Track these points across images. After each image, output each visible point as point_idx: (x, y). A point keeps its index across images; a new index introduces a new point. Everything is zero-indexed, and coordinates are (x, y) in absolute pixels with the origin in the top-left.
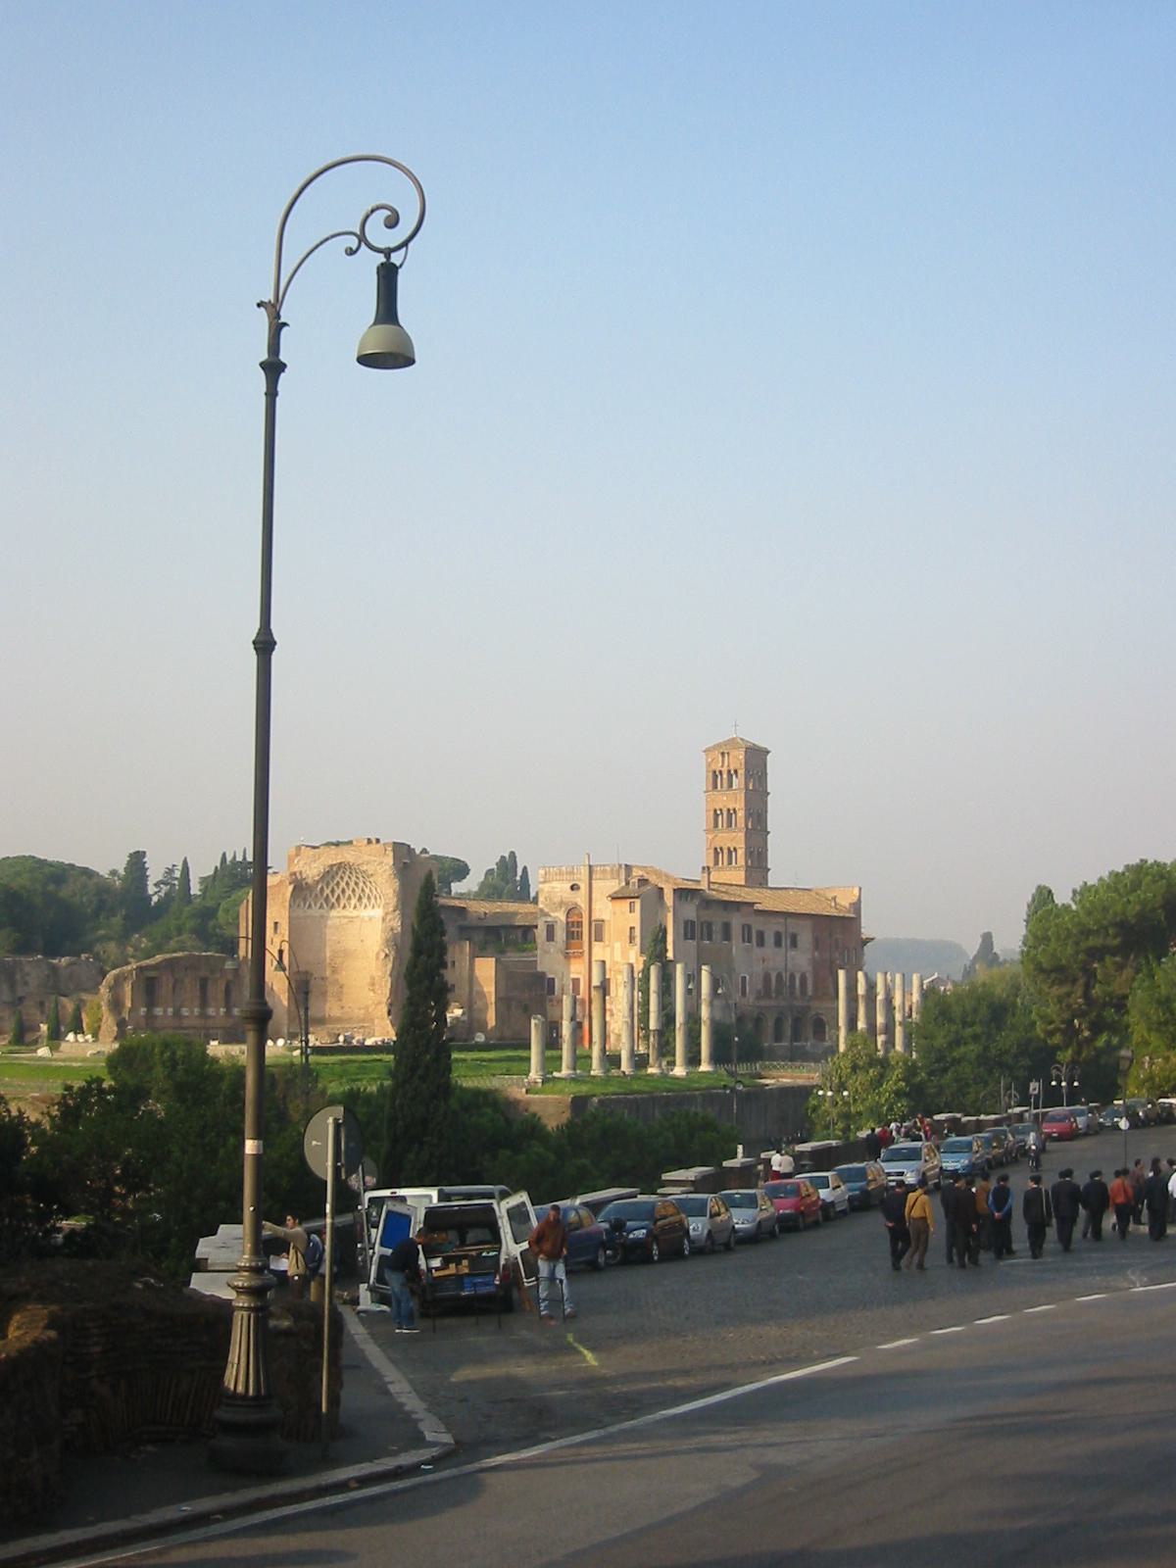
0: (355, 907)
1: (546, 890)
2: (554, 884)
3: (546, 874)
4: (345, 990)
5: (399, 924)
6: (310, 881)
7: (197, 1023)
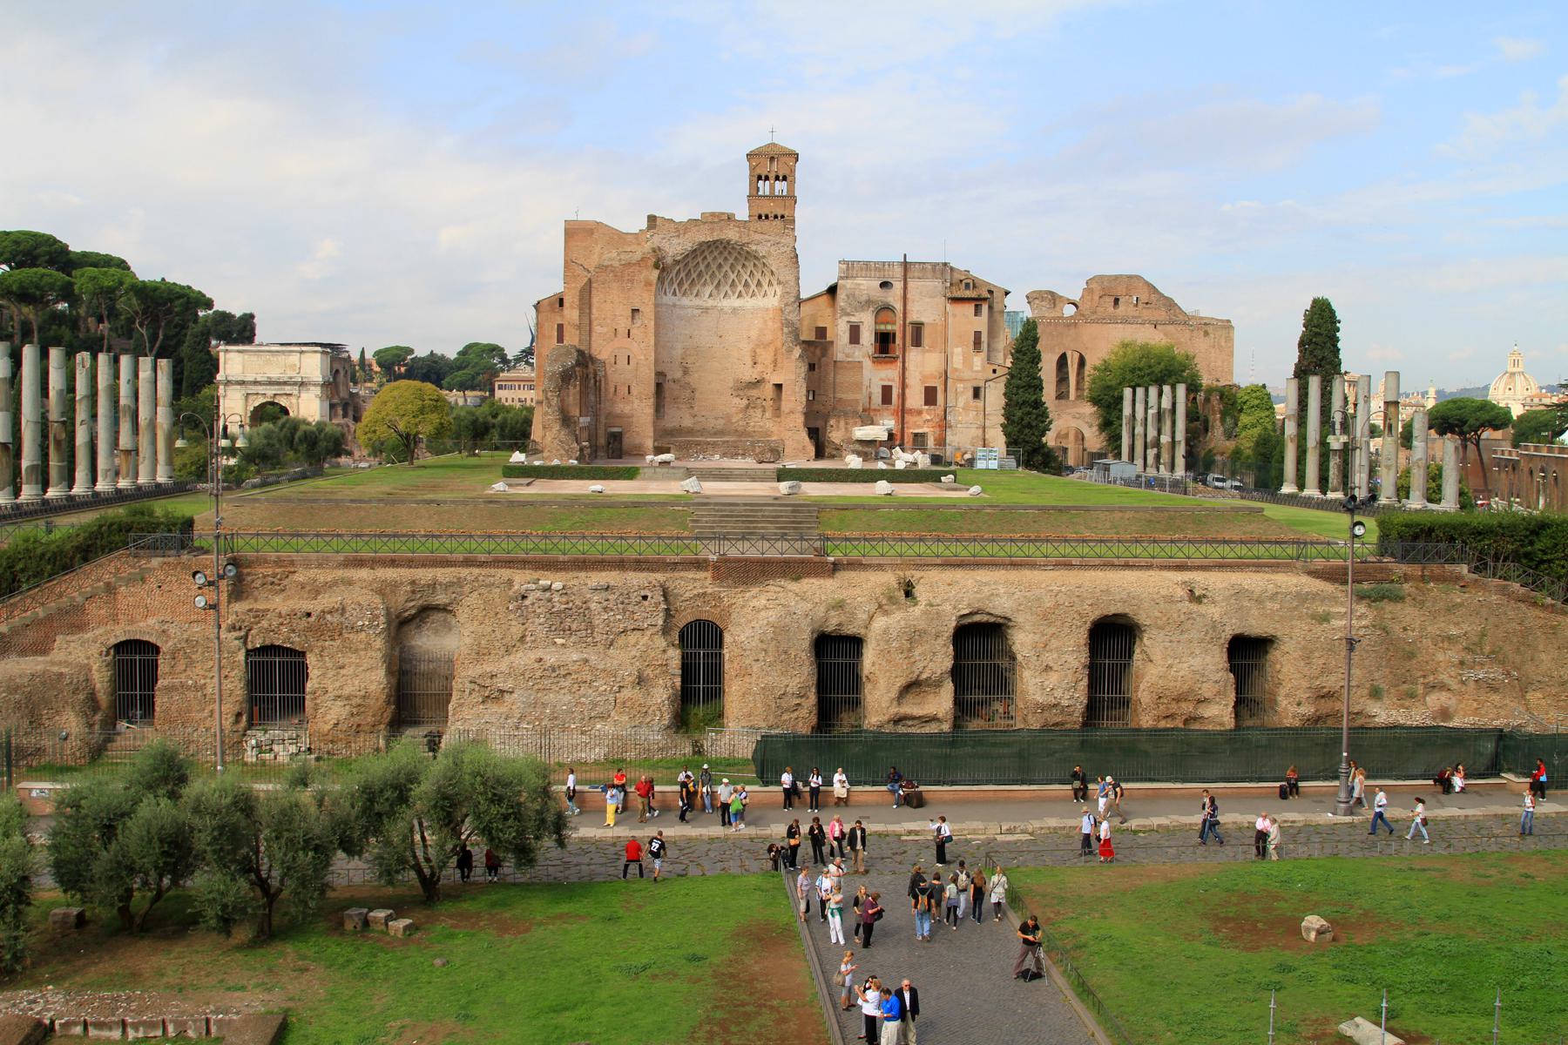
0: (710, 295)
1: (848, 286)
2: (859, 281)
3: (848, 269)
4: (697, 395)
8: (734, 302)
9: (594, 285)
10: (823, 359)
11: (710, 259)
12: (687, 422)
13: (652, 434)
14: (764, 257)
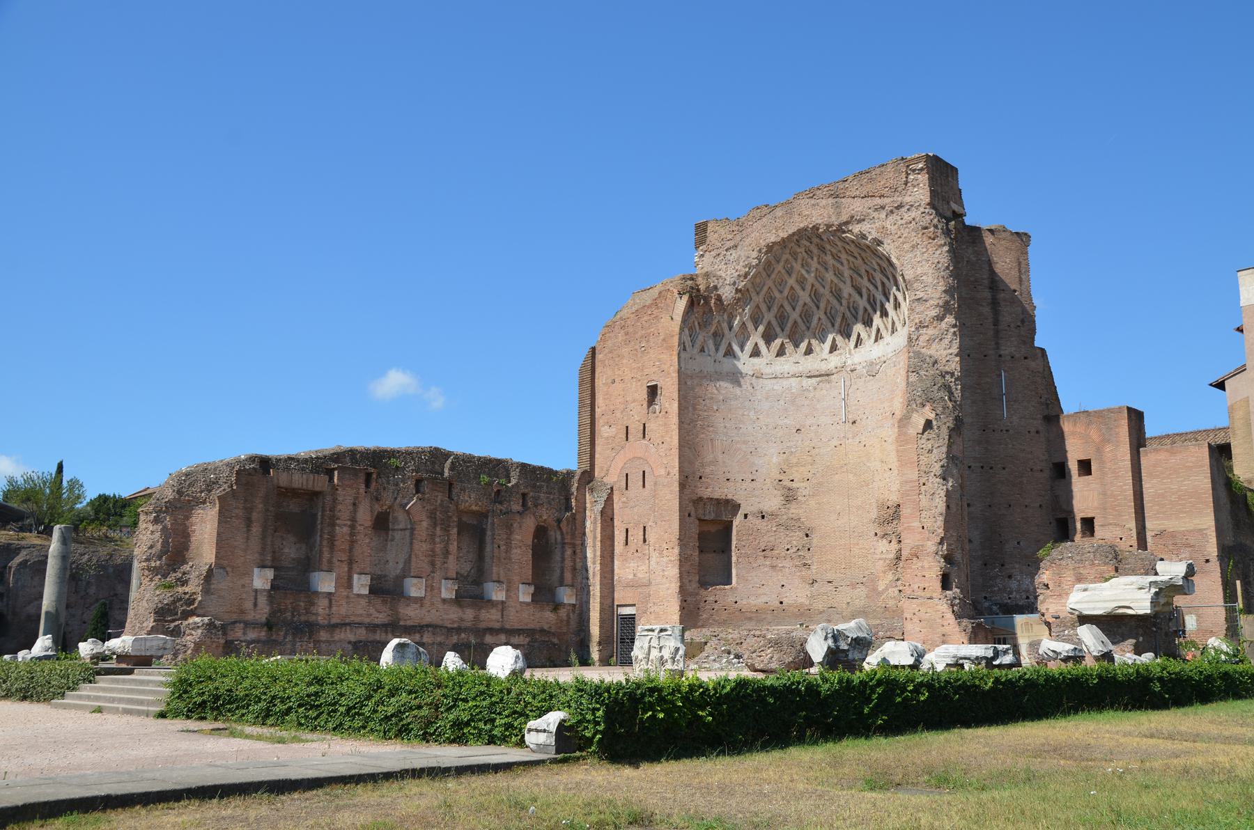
0: (834, 348)
4: (815, 541)
5: (955, 350)
6: (727, 293)
7: (452, 615)
8: (871, 351)
9: (599, 357)
10: (1108, 448)
11: (811, 278)
12: (797, 594)
13: (676, 617)
14: (880, 243)
